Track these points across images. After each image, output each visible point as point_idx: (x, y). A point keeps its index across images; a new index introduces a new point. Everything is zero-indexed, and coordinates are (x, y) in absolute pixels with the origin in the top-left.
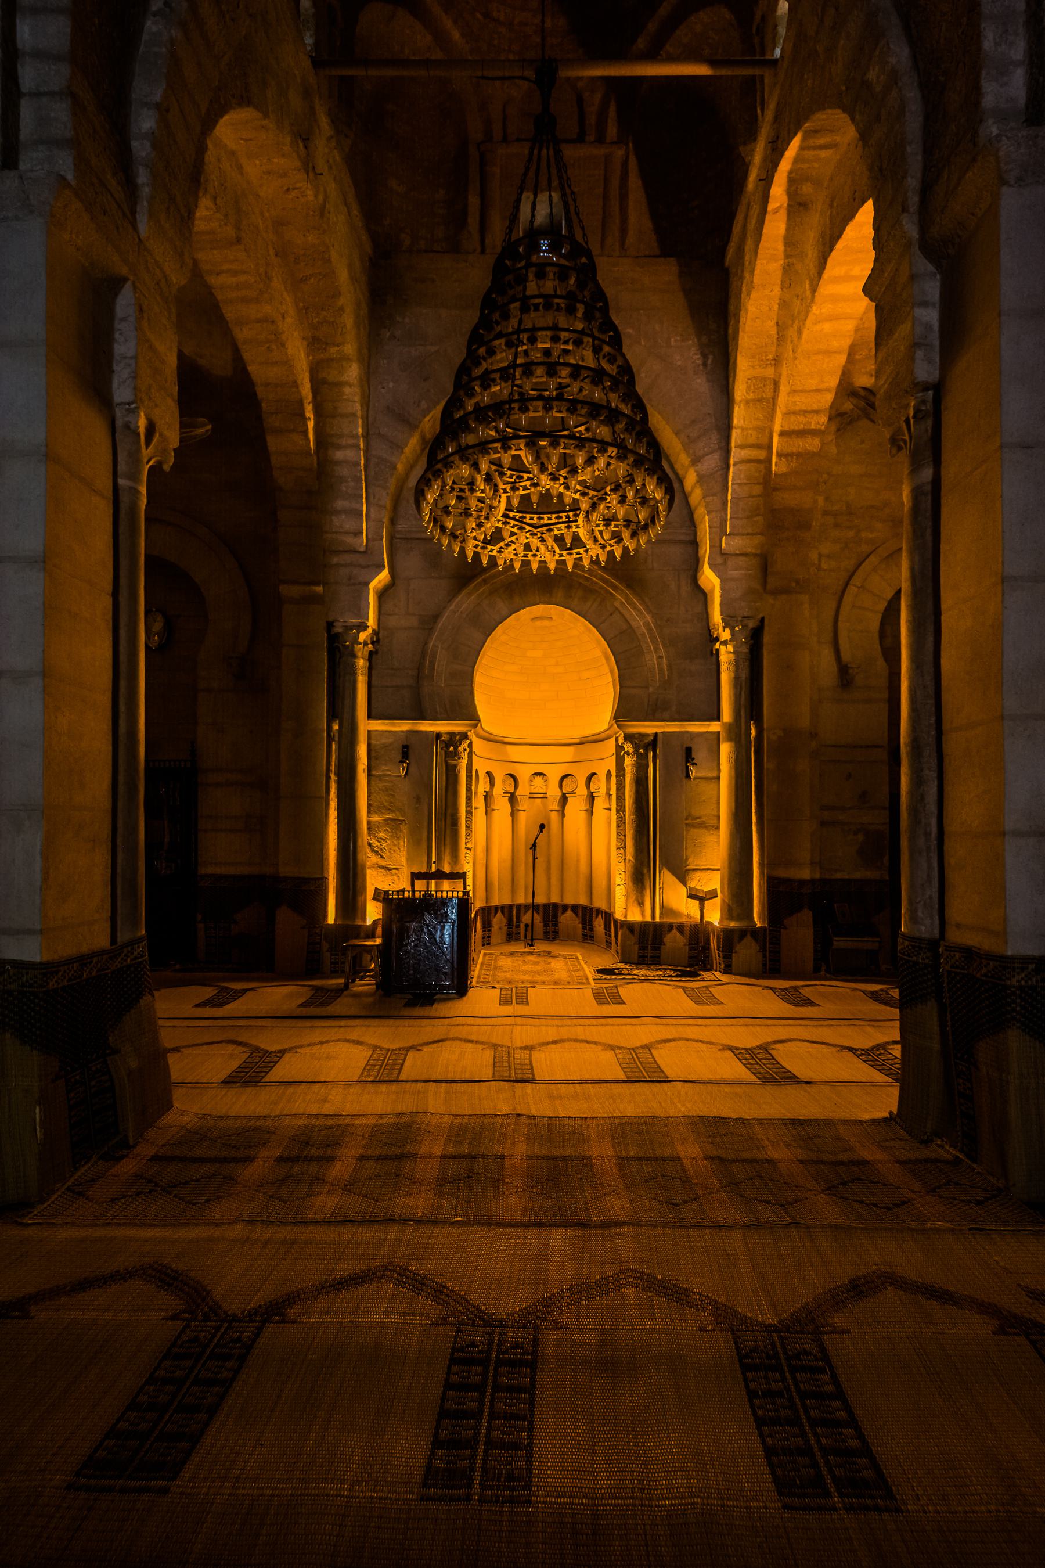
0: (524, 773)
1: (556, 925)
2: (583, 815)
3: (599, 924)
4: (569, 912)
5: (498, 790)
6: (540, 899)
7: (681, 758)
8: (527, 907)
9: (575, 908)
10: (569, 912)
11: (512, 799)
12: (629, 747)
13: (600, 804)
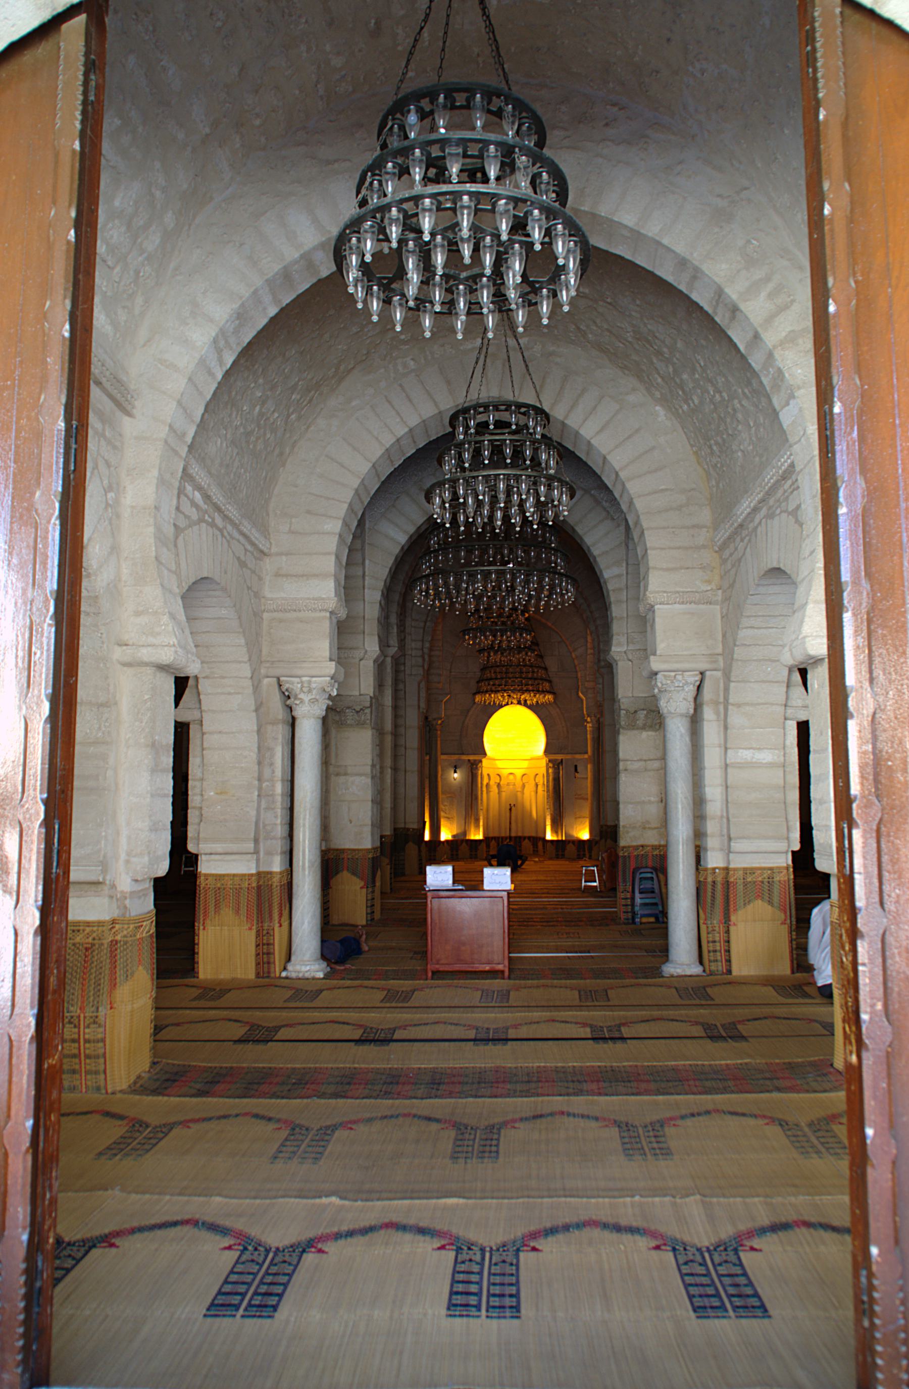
0: (505, 772)
1: (520, 847)
2: (533, 794)
3: (540, 844)
4: (527, 841)
5: (492, 783)
6: (513, 834)
7: (573, 769)
8: (506, 838)
9: (529, 838)
10: (527, 841)
11: (499, 785)
12: (551, 765)
13: (540, 788)
